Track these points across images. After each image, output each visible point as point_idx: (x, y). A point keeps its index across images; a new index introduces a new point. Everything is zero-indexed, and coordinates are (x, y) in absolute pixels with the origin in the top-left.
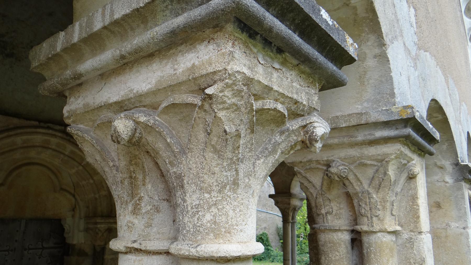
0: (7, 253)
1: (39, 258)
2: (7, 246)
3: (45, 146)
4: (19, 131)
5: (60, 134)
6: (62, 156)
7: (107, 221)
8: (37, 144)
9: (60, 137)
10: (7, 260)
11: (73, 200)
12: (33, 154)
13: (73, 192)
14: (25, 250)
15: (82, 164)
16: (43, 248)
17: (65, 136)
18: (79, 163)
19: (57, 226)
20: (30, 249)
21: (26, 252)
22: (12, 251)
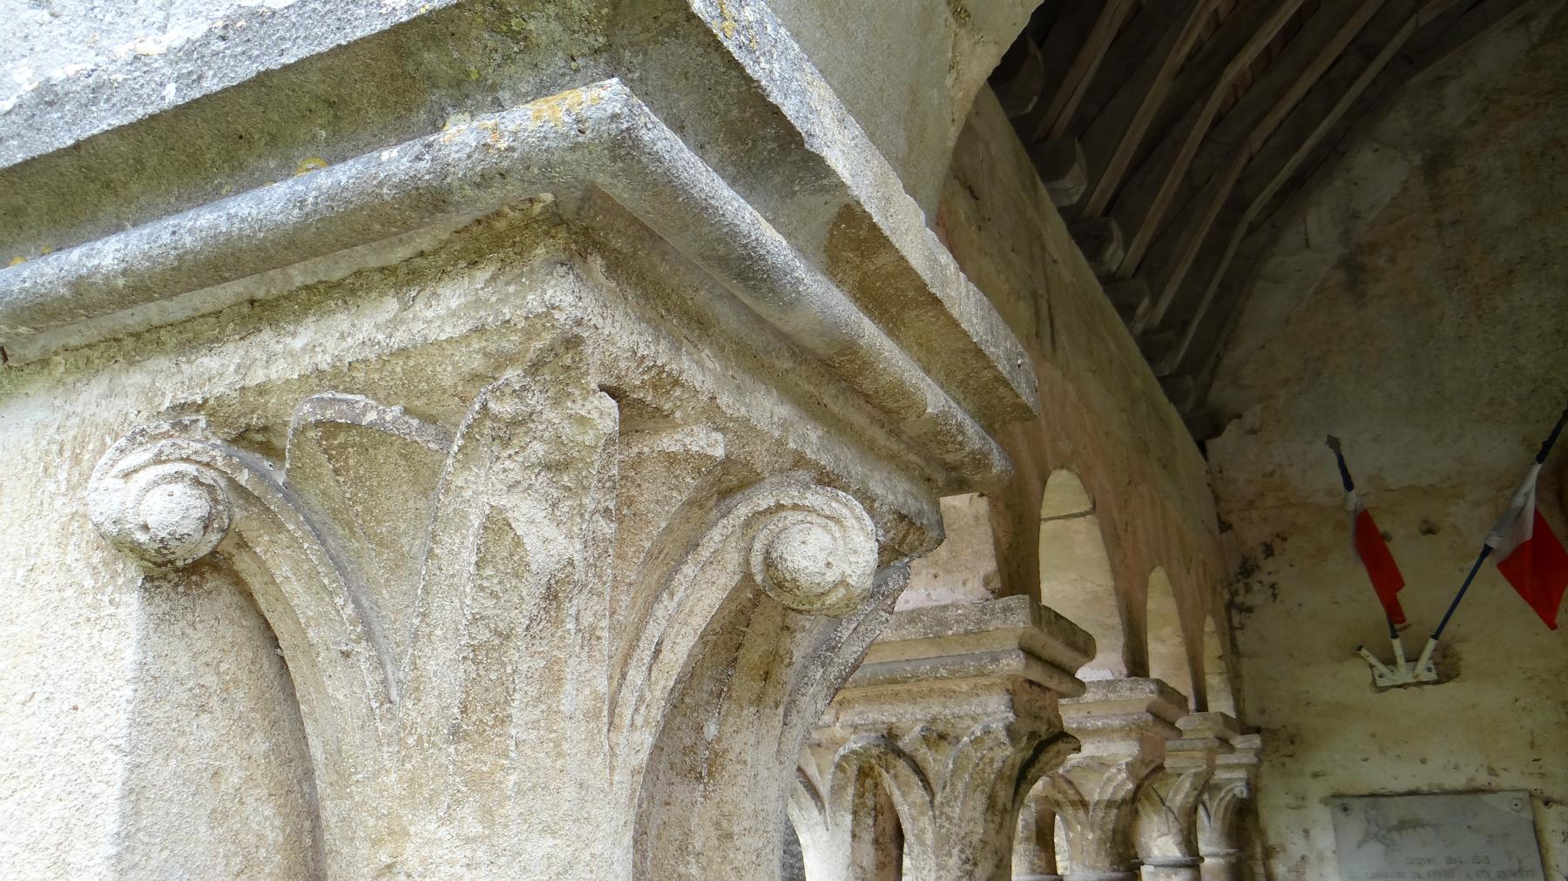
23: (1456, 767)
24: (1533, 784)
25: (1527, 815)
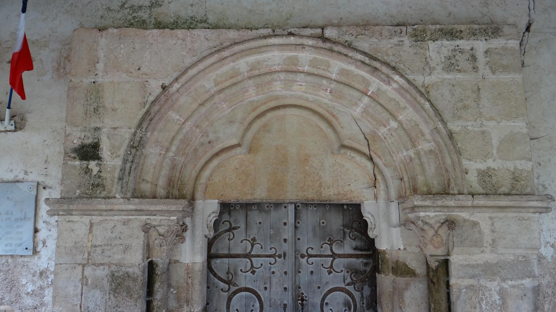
0: (272, 260)
1: (330, 273)
2: (271, 249)
3: (291, 70)
4: (237, 48)
5: (310, 42)
6: (324, 82)
7: (439, 203)
8: (277, 68)
9: (312, 46)
10: (273, 273)
11: (369, 165)
12: (278, 88)
13: (366, 151)
14: (303, 256)
15: (369, 94)
16: (334, 256)
17: (320, 44)
18: (363, 92)
19: (353, 217)
20: (311, 256)
21: (304, 261)
22: (280, 256)
23: (11, 171)
24: (41, 179)
25: (34, 193)
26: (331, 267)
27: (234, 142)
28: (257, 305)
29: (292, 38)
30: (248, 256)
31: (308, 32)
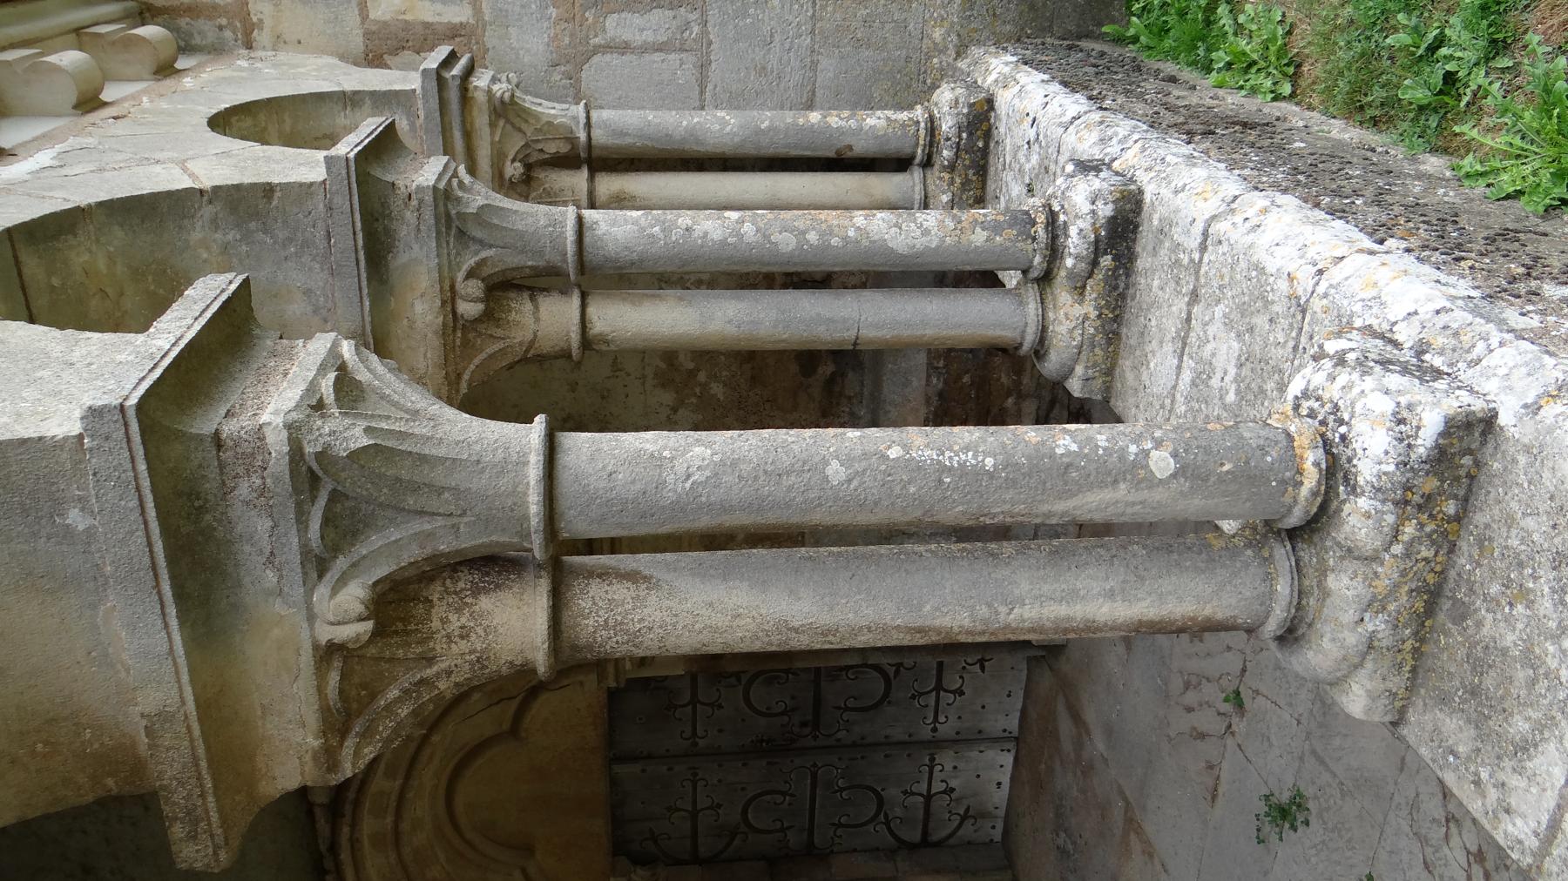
1: (720, 707)
5: (346, 830)
6: (410, 795)
11: (544, 697)
16: (694, 702)
17: (347, 819)
21: (701, 743)
26: (711, 705)
27: (517, 874)
28: (768, 797)
29: (342, 856)
30: (694, 815)
31: (323, 826)
